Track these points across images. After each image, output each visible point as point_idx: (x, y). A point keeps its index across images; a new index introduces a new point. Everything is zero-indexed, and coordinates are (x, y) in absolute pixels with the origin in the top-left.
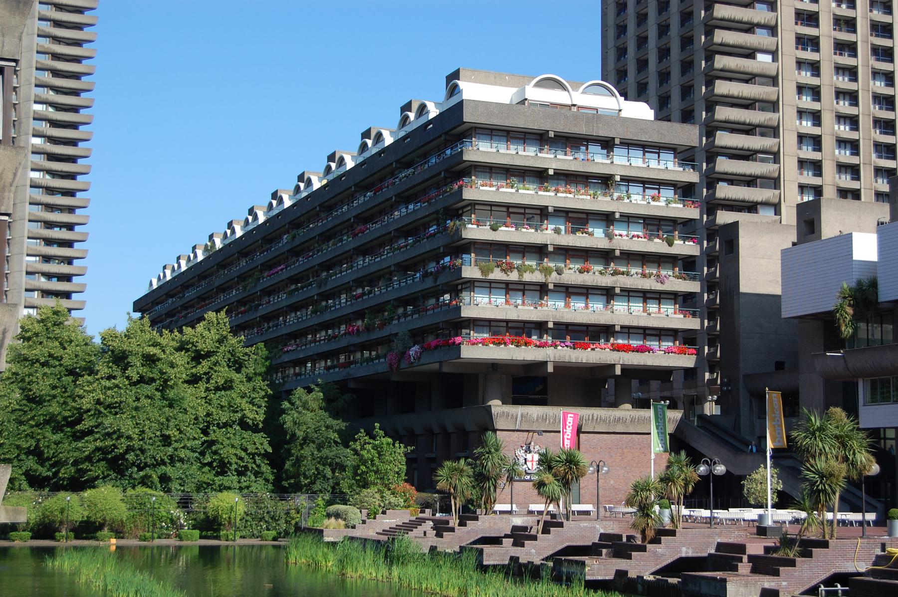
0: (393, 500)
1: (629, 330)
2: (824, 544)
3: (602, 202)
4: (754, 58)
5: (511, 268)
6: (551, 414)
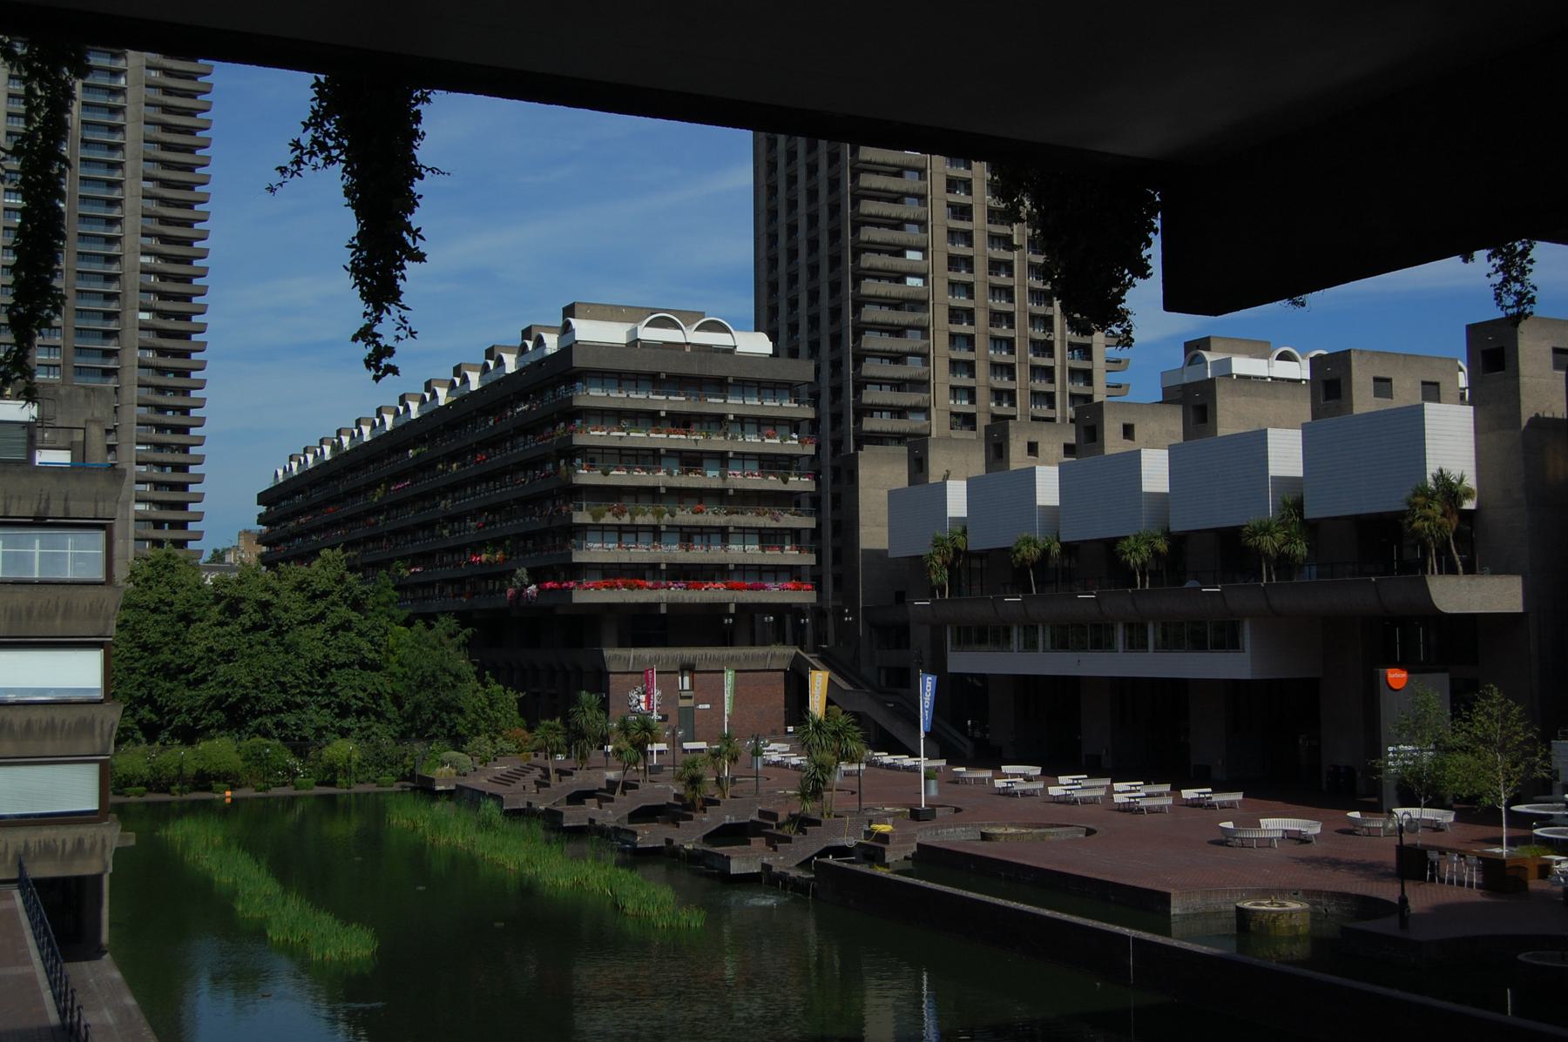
0: (506, 746)
1: (743, 569)
2: (817, 823)
3: (717, 442)
4: (904, 255)
5: (623, 512)
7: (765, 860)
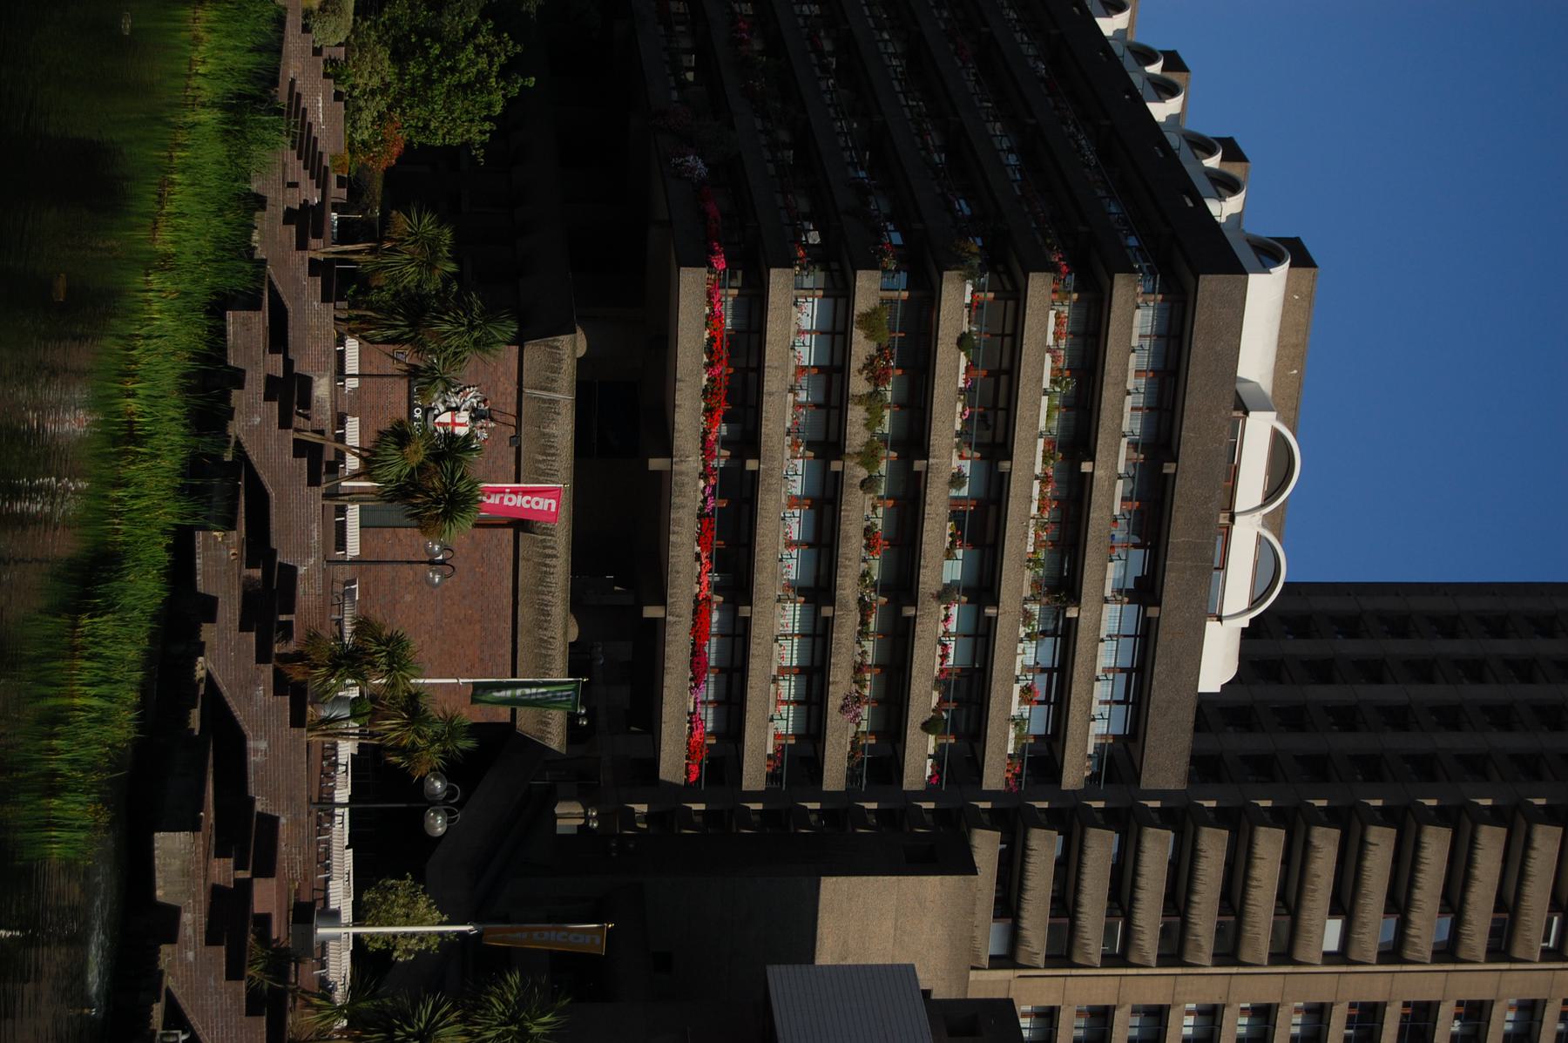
0: (367, 116)
1: (739, 636)
3: (1019, 581)
4: (1333, 913)
5: (877, 376)
6: (556, 465)
7: (187, 918)
